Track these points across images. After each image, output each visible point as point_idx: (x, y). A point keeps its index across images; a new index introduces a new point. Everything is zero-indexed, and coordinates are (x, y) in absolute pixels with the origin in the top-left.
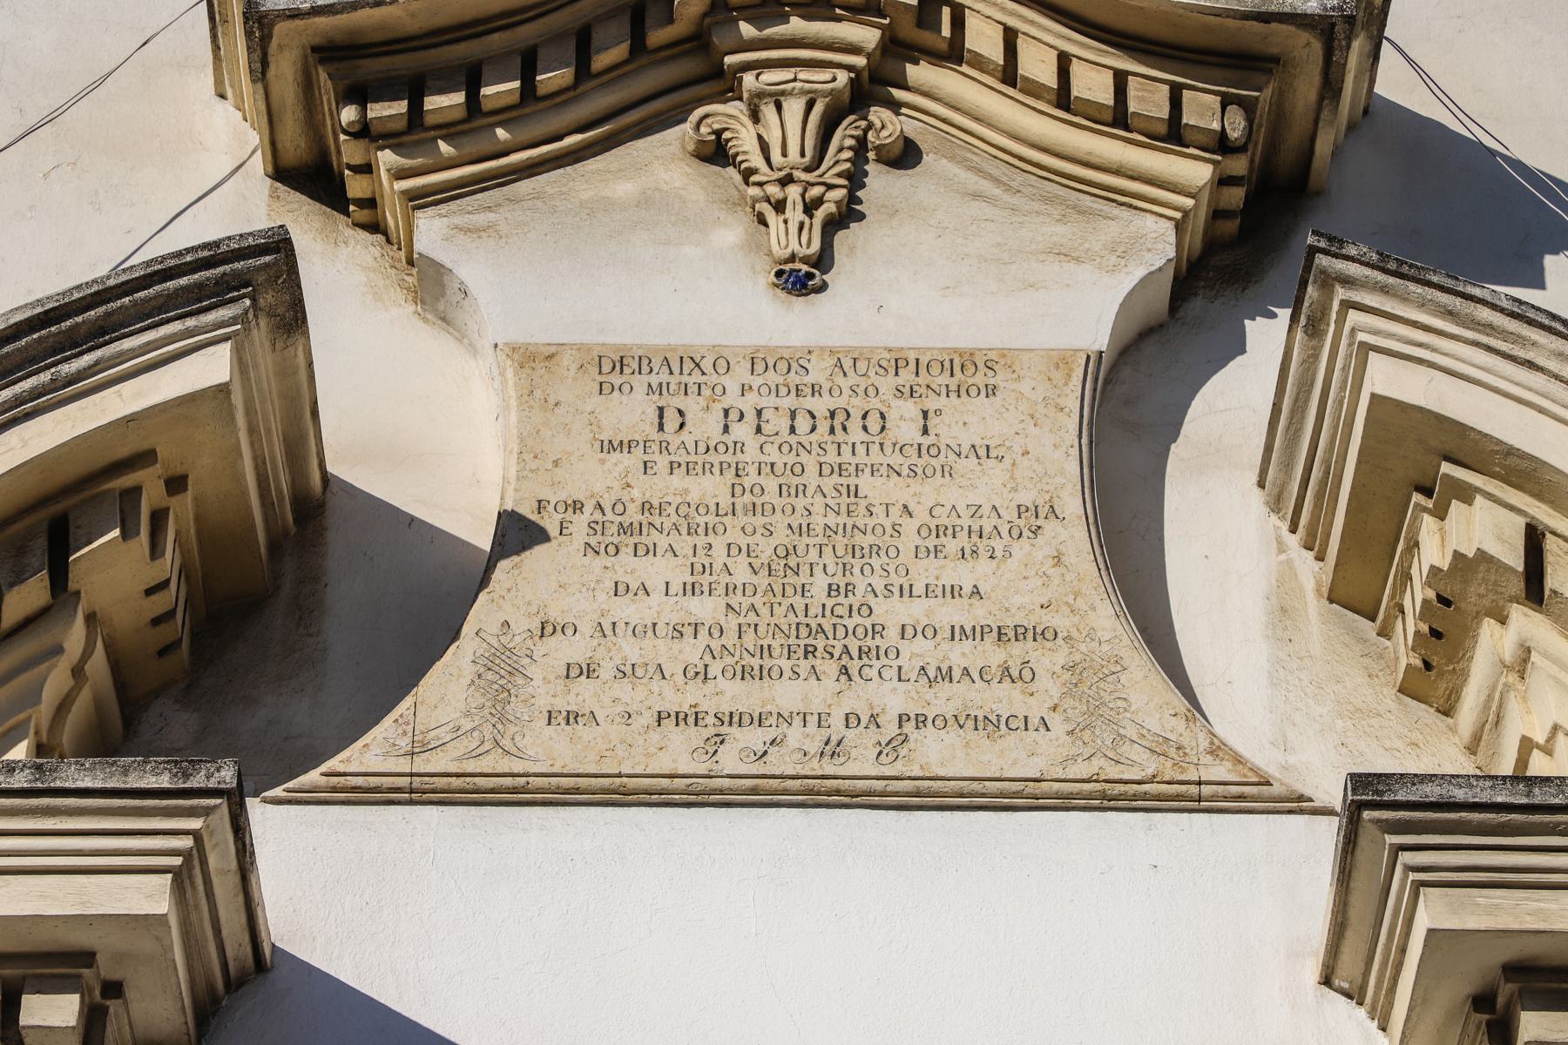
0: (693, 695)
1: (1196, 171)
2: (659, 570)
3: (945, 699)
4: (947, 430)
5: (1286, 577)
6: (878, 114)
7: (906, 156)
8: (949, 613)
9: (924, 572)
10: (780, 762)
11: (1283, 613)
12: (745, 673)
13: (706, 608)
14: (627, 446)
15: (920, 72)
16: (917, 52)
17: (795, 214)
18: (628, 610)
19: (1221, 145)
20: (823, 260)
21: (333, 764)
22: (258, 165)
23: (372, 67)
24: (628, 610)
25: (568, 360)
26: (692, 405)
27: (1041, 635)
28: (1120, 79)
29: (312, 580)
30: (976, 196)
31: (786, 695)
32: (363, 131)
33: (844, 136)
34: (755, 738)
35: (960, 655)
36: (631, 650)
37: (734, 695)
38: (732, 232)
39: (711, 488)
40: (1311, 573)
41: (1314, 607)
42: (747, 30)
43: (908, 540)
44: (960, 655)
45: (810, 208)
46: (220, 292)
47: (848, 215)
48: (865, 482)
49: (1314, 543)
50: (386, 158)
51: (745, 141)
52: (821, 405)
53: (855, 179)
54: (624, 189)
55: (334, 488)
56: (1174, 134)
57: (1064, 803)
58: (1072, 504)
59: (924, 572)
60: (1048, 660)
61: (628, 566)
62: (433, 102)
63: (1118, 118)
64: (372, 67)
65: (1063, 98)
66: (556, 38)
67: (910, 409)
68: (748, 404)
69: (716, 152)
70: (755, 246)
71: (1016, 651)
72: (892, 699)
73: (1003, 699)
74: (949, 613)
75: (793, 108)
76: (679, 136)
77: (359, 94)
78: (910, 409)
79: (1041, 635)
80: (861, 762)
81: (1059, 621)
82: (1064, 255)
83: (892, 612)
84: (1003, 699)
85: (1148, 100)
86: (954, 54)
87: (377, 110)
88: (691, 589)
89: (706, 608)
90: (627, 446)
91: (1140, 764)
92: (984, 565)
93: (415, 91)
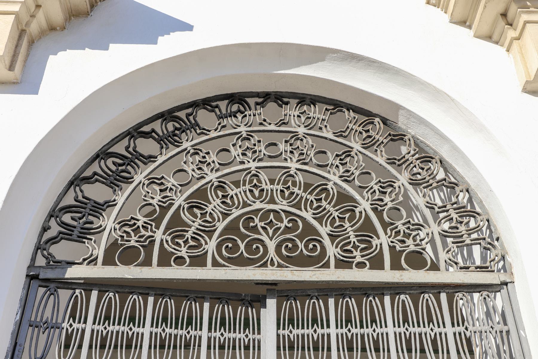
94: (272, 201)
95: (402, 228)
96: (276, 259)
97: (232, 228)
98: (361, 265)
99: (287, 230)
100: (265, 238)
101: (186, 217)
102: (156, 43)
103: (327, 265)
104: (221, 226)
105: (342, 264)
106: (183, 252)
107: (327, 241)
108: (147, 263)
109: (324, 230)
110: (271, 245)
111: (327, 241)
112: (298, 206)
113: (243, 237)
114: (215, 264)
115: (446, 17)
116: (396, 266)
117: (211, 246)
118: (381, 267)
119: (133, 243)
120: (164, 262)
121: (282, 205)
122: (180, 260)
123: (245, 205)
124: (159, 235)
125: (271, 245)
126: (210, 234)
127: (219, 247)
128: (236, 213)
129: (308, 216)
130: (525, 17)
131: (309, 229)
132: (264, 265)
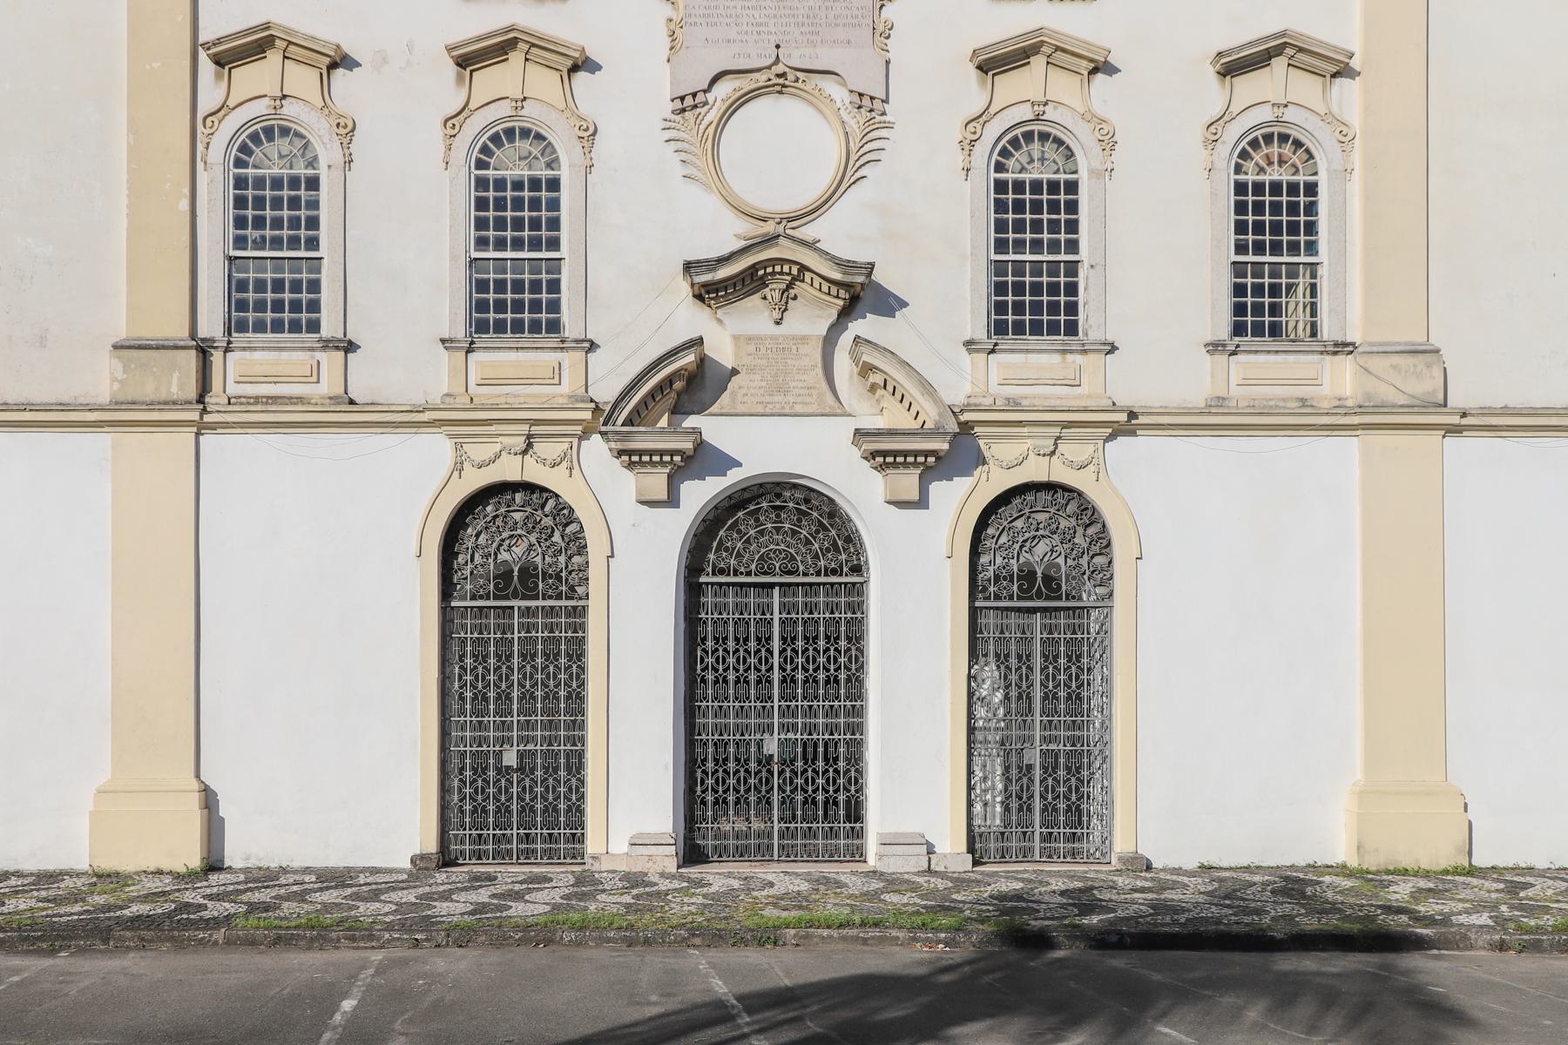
0: (763, 399)
1: (841, 303)
2: (757, 377)
3: (799, 399)
4: (801, 351)
5: (852, 371)
6: (791, 291)
7: (795, 298)
8: (801, 384)
9: (797, 377)
10: (775, 411)
11: (851, 377)
12: (770, 395)
13: (764, 384)
14: (751, 355)
15: (797, 283)
16: (797, 280)
17: (777, 309)
18: (752, 384)
19: (845, 299)
20: (781, 319)
21: (709, 410)
22: (691, 294)
23: (709, 288)
24: (752, 384)
25: (742, 338)
26: (761, 347)
27: (814, 388)
28: (829, 287)
29: (703, 377)
30: (806, 305)
31: (776, 399)
32: (709, 298)
33: (785, 295)
34: (771, 406)
35: (802, 392)
36: (753, 391)
37: (768, 399)
38: (767, 313)
39: (764, 362)
40: (856, 370)
41: (856, 376)
42: (769, 277)
43: (794, 372)
44: (802, 392)
45: (779, 309)
46: (692, 346)
47: (786, 310)
48: (789, 361)
49: (857, 365)
50: (713, 302)
51: (769, 297)
52: (781, 347)
53: (787, 303)
54: (750, 305)
55: (707, 364)
56: (837, 297)
57: (817, 416)
58: (820, 365)
59: (797, 377)
60: (815, 392)
61: (752, 376)
62: (720, 294)
63: (829, 294)
64: (709, 288)
65: (820, 290)
66: (739, 281)
67: (794, 347)
68: (769, 346)
69: (765, 298)
70: (771, 315)
71: (810, 391)
72: (792, 399)
73: (807, 399)
74: (801, 384)
75: (777, 291)
76: (758, 295)
77: (708, 293)
78: (794, 347)
79: (814, 388)
80: (787, 411)
81: (817, 386)
82: (819, 317)
83: (792, 384)
84: (807, 399)
85: (834, 290)
86: (803, 281)
87: (711, 296)
88: (762, 380)
89: (764, 384)
90: (751, 355)
91: (828, 410)
92: (806, 376)
93: (717, 291)
94: (778, 544)
95: (830, 557)
96: (780, 572)
97: (761, 558)
98: (812, 574)
99: (784, 559)
100: (775, 563)
101: (742, 552)
102: (726, 476)
103: (799, 575)
104: (757, 557)
105: (805, 574)
106: (742, 569)
107: (800, 564)
108: (729, 575)
109: (799, 558)
110: (778, 565)
111: (800, 564)
112: (788, 547)
113: (766, 562)
114: (756, 575)
115: (859, 454)
116: (826, 575)
117: (753, 567)
118: (820, 575)
119: (722, 566)
120: (735, 574)
121: (782, 547)
122: (742, 573)
123: (767, 547)
124: (732, 562)
125: (778, 565)
126: (753, 561)
127: (756, 567)
128: (763, 551)
129: (792, 551)
130: (888, 472)
131: (793, 558)
132: (774, 575)
